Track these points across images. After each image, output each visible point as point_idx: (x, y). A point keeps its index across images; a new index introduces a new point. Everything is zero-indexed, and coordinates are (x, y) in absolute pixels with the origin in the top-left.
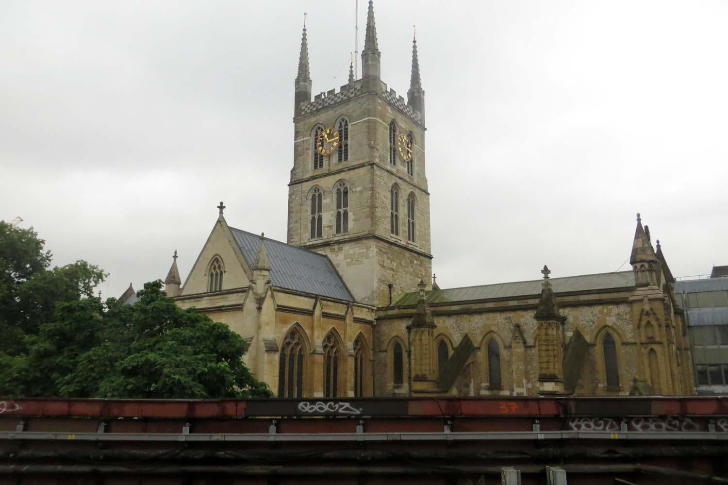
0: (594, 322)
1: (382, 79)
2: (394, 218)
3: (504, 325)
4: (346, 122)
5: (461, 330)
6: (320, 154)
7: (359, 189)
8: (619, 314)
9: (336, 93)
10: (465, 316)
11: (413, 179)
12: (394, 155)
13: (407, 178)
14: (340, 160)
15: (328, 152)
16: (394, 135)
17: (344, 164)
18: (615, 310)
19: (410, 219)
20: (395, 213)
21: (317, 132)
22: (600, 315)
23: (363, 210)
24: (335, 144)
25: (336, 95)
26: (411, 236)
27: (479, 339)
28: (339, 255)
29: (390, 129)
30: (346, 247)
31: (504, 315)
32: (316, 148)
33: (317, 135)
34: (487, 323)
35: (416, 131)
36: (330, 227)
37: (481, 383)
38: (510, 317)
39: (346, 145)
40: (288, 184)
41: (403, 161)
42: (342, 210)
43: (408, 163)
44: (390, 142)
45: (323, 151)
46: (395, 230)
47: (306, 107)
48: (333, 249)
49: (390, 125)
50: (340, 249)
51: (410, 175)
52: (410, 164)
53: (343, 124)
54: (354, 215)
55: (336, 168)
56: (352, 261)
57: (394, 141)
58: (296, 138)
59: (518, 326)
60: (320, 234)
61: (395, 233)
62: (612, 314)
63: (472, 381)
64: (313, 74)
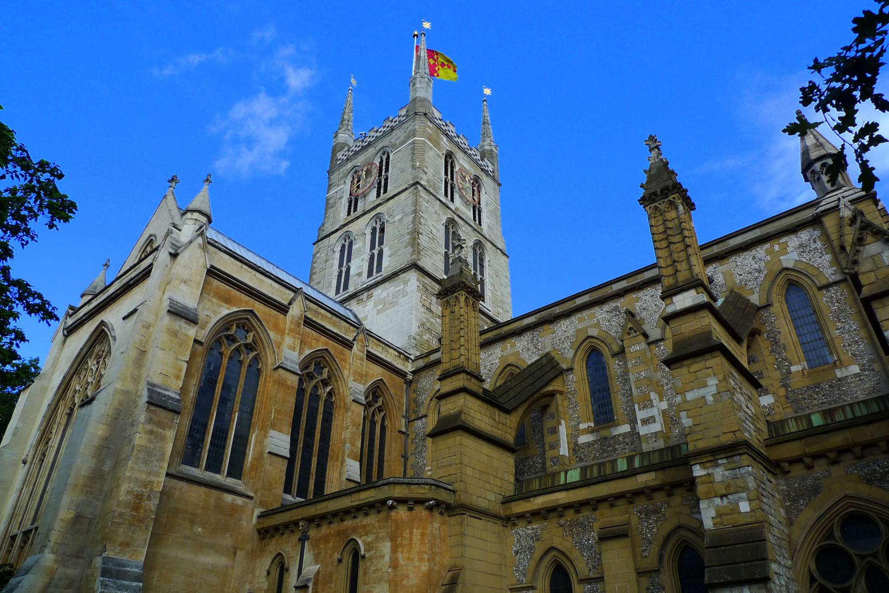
0: (760, 271)
3: (609, 321)
5: (539, 350)
7: (397, 218)
8: (801, 245)
10: (546, 327)
18: (793, 241)
22: (769, 258)
23: (401, 241)
27: (570, 354)
28: (368, 304)
30: (377, 292)
31: (606, 307)
34: (580, 326)
36: (359, 275)
37: (578, 424)
38: (618, 307)
48: (360, 300)
50: (369, 297)
54: (390, 249)
55: (372, 206)
56: (383, 306)
59: (631, 314)
62: (789, 249)
63: (563, 422)
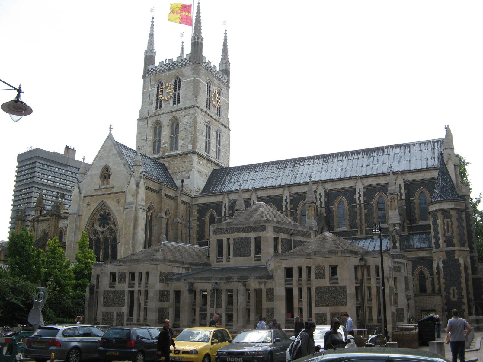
1: (203, 55)
2: (208, 143)
4: (180, 79)
6: (160, 99)
9: (173, 61)
11: (220, 119)
12: (209, 103)
13: (217, 119)
14: (174, 104)
15: (166, 98)
16: (210, 90)
17: (176, 107)
19: (218, 145)
20: (208, 139)
21: (159, 85)
24: (171, 94)
25: (173, 63)
26: (218, 156)
29: (208, 86)
32: (157, 95)
33: (158, 87)
35: (224, 89)
39: (179, 94)
40: (138, 119)
41: (214, 107)
42: (174, 136)
43: (217, 108)
44: (207, 94)
45: (163, 98)
46: (208, 149)
47: (152, 69)
49: (208, 83)
51: (218, 116)
52: (219, 110)
53: (177, 81)
57: (209, 94)
58: (144, 89)
60: (159, 152)
61: (207, 151)
64: (156, 48)
